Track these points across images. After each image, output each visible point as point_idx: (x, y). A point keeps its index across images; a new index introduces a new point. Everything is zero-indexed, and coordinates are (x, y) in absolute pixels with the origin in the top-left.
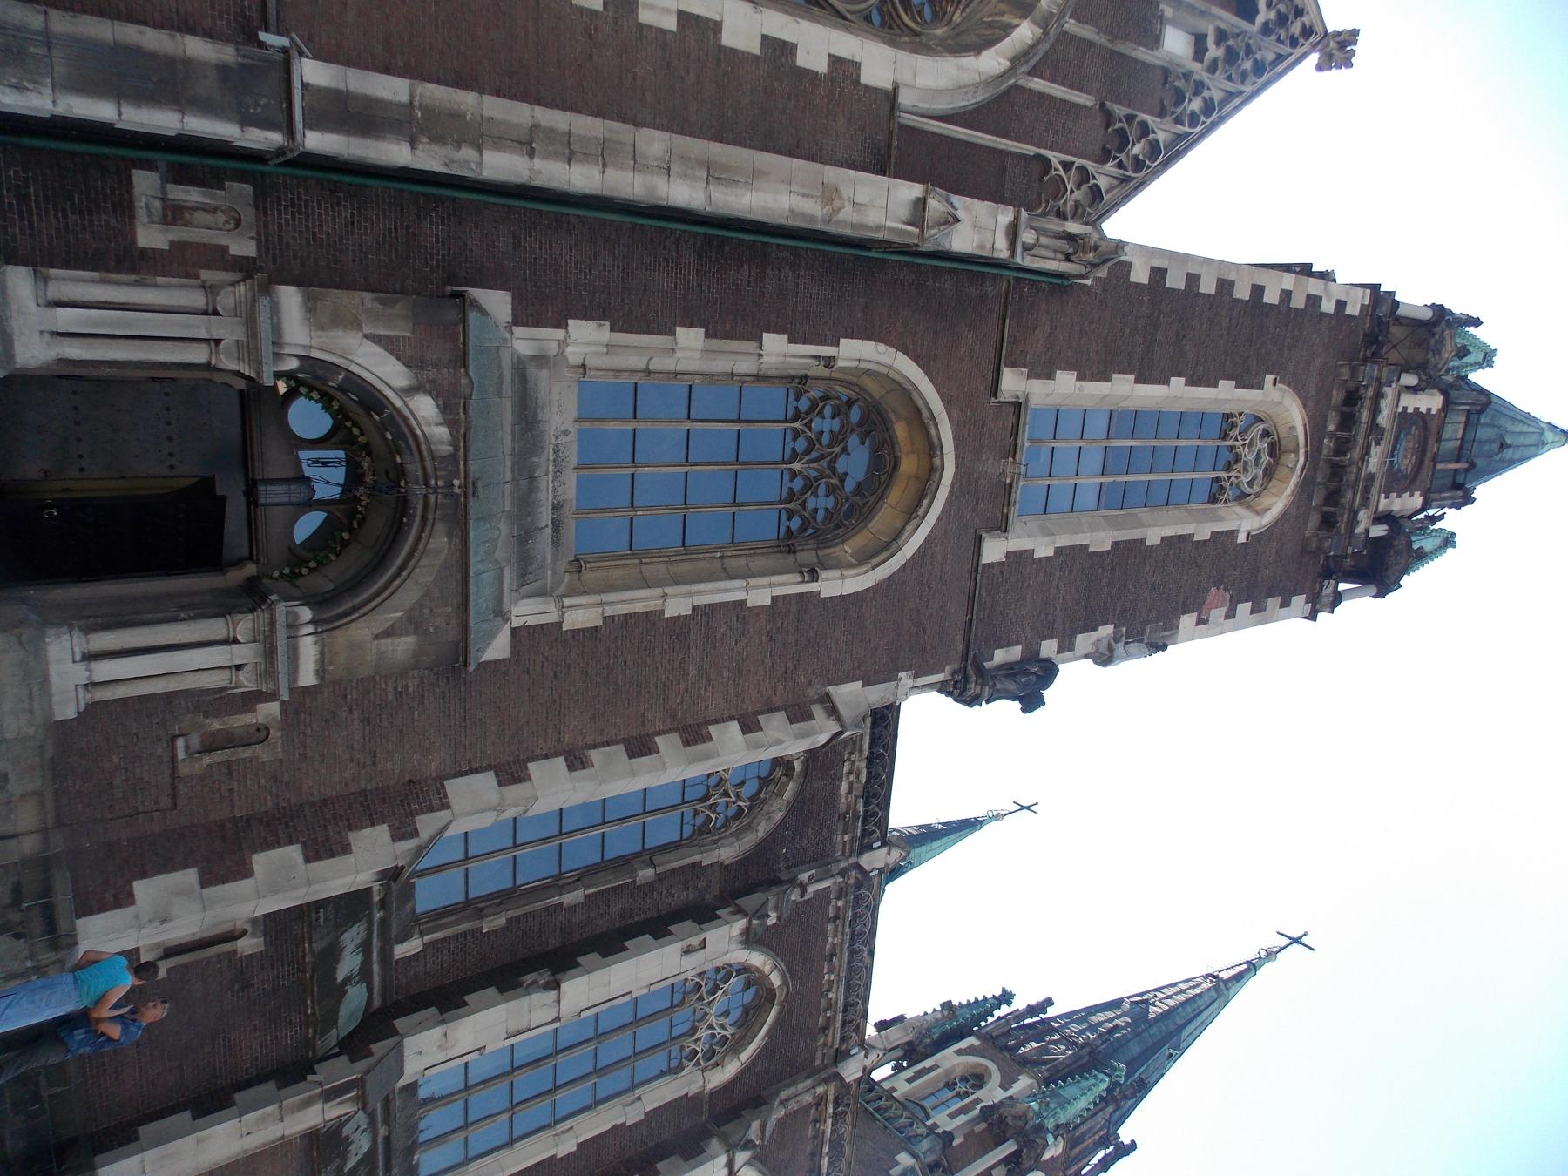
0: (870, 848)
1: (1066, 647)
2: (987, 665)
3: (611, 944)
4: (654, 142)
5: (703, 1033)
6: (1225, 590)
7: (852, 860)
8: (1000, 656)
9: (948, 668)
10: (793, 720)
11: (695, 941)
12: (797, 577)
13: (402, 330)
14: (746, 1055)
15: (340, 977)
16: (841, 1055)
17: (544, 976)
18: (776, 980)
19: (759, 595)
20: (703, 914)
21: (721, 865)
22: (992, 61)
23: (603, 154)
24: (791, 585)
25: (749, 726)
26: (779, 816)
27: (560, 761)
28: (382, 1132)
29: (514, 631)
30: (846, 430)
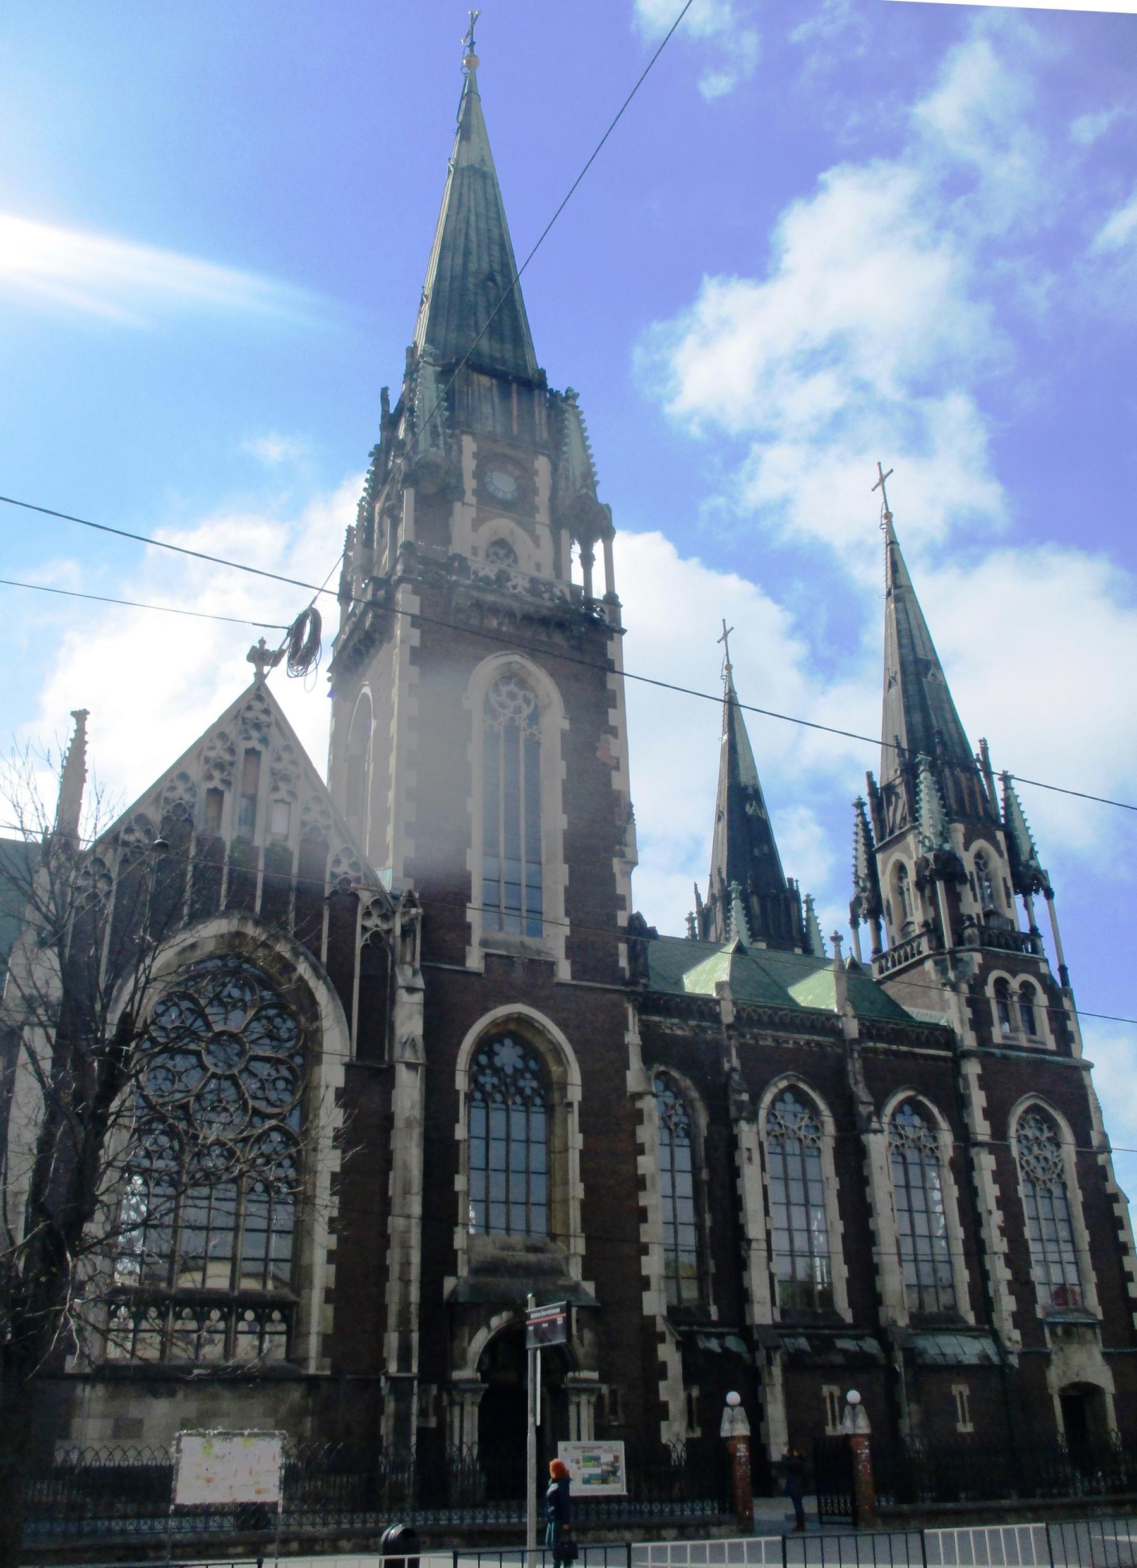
0: (719, 1014)
1: (622, 902)
2: (627, 974)
3: (736, 1203)
4: (396, 1224)
5: (802, 1133)
6: (598, 740)
7: (724, 1029)
8: (623, 962)
9: (626, 1005)
10: (641, 1122)
11: (745, 1154)
12: (570, 1117)
13: (466, 1330)
14: (821, 1105)
15: (719, 1350)
16: (839, 1033)
17: (744, 1244)
18: (783, 1084)
19: (577, 1141)
20: (733, 1143)
21: (709, 1125)
22: (322, 993)
23: (405, 1247)
24: (574, 1120)
25: (641, 1150)
26: (689, 1082)
27: (644, 1258)
28: (800, 1330)
29: (585, 1278)
30: (491, 1065)
